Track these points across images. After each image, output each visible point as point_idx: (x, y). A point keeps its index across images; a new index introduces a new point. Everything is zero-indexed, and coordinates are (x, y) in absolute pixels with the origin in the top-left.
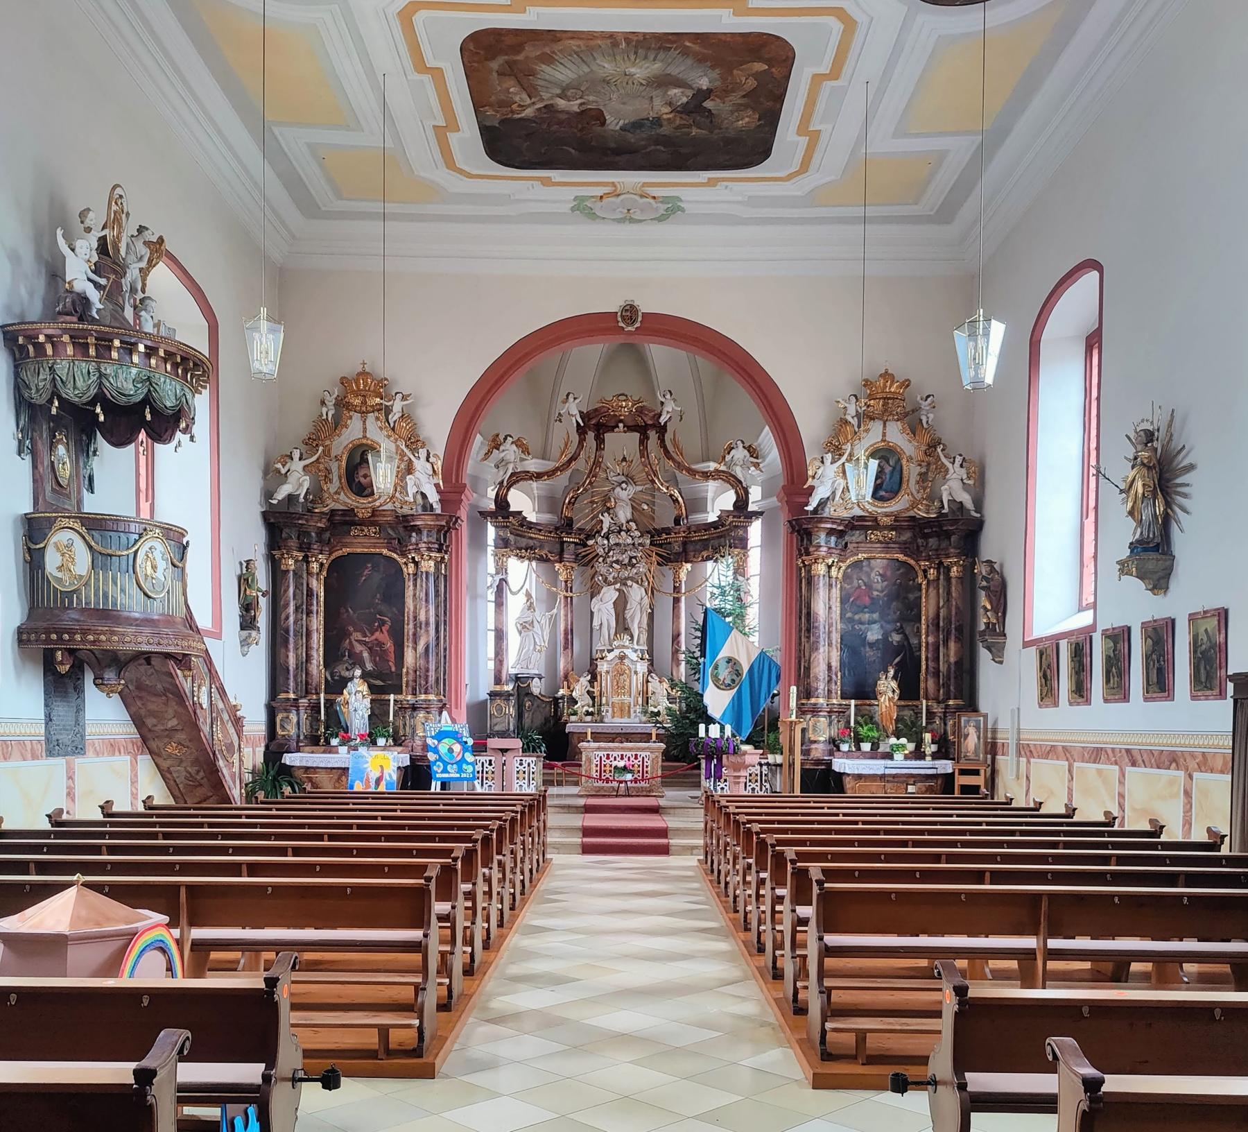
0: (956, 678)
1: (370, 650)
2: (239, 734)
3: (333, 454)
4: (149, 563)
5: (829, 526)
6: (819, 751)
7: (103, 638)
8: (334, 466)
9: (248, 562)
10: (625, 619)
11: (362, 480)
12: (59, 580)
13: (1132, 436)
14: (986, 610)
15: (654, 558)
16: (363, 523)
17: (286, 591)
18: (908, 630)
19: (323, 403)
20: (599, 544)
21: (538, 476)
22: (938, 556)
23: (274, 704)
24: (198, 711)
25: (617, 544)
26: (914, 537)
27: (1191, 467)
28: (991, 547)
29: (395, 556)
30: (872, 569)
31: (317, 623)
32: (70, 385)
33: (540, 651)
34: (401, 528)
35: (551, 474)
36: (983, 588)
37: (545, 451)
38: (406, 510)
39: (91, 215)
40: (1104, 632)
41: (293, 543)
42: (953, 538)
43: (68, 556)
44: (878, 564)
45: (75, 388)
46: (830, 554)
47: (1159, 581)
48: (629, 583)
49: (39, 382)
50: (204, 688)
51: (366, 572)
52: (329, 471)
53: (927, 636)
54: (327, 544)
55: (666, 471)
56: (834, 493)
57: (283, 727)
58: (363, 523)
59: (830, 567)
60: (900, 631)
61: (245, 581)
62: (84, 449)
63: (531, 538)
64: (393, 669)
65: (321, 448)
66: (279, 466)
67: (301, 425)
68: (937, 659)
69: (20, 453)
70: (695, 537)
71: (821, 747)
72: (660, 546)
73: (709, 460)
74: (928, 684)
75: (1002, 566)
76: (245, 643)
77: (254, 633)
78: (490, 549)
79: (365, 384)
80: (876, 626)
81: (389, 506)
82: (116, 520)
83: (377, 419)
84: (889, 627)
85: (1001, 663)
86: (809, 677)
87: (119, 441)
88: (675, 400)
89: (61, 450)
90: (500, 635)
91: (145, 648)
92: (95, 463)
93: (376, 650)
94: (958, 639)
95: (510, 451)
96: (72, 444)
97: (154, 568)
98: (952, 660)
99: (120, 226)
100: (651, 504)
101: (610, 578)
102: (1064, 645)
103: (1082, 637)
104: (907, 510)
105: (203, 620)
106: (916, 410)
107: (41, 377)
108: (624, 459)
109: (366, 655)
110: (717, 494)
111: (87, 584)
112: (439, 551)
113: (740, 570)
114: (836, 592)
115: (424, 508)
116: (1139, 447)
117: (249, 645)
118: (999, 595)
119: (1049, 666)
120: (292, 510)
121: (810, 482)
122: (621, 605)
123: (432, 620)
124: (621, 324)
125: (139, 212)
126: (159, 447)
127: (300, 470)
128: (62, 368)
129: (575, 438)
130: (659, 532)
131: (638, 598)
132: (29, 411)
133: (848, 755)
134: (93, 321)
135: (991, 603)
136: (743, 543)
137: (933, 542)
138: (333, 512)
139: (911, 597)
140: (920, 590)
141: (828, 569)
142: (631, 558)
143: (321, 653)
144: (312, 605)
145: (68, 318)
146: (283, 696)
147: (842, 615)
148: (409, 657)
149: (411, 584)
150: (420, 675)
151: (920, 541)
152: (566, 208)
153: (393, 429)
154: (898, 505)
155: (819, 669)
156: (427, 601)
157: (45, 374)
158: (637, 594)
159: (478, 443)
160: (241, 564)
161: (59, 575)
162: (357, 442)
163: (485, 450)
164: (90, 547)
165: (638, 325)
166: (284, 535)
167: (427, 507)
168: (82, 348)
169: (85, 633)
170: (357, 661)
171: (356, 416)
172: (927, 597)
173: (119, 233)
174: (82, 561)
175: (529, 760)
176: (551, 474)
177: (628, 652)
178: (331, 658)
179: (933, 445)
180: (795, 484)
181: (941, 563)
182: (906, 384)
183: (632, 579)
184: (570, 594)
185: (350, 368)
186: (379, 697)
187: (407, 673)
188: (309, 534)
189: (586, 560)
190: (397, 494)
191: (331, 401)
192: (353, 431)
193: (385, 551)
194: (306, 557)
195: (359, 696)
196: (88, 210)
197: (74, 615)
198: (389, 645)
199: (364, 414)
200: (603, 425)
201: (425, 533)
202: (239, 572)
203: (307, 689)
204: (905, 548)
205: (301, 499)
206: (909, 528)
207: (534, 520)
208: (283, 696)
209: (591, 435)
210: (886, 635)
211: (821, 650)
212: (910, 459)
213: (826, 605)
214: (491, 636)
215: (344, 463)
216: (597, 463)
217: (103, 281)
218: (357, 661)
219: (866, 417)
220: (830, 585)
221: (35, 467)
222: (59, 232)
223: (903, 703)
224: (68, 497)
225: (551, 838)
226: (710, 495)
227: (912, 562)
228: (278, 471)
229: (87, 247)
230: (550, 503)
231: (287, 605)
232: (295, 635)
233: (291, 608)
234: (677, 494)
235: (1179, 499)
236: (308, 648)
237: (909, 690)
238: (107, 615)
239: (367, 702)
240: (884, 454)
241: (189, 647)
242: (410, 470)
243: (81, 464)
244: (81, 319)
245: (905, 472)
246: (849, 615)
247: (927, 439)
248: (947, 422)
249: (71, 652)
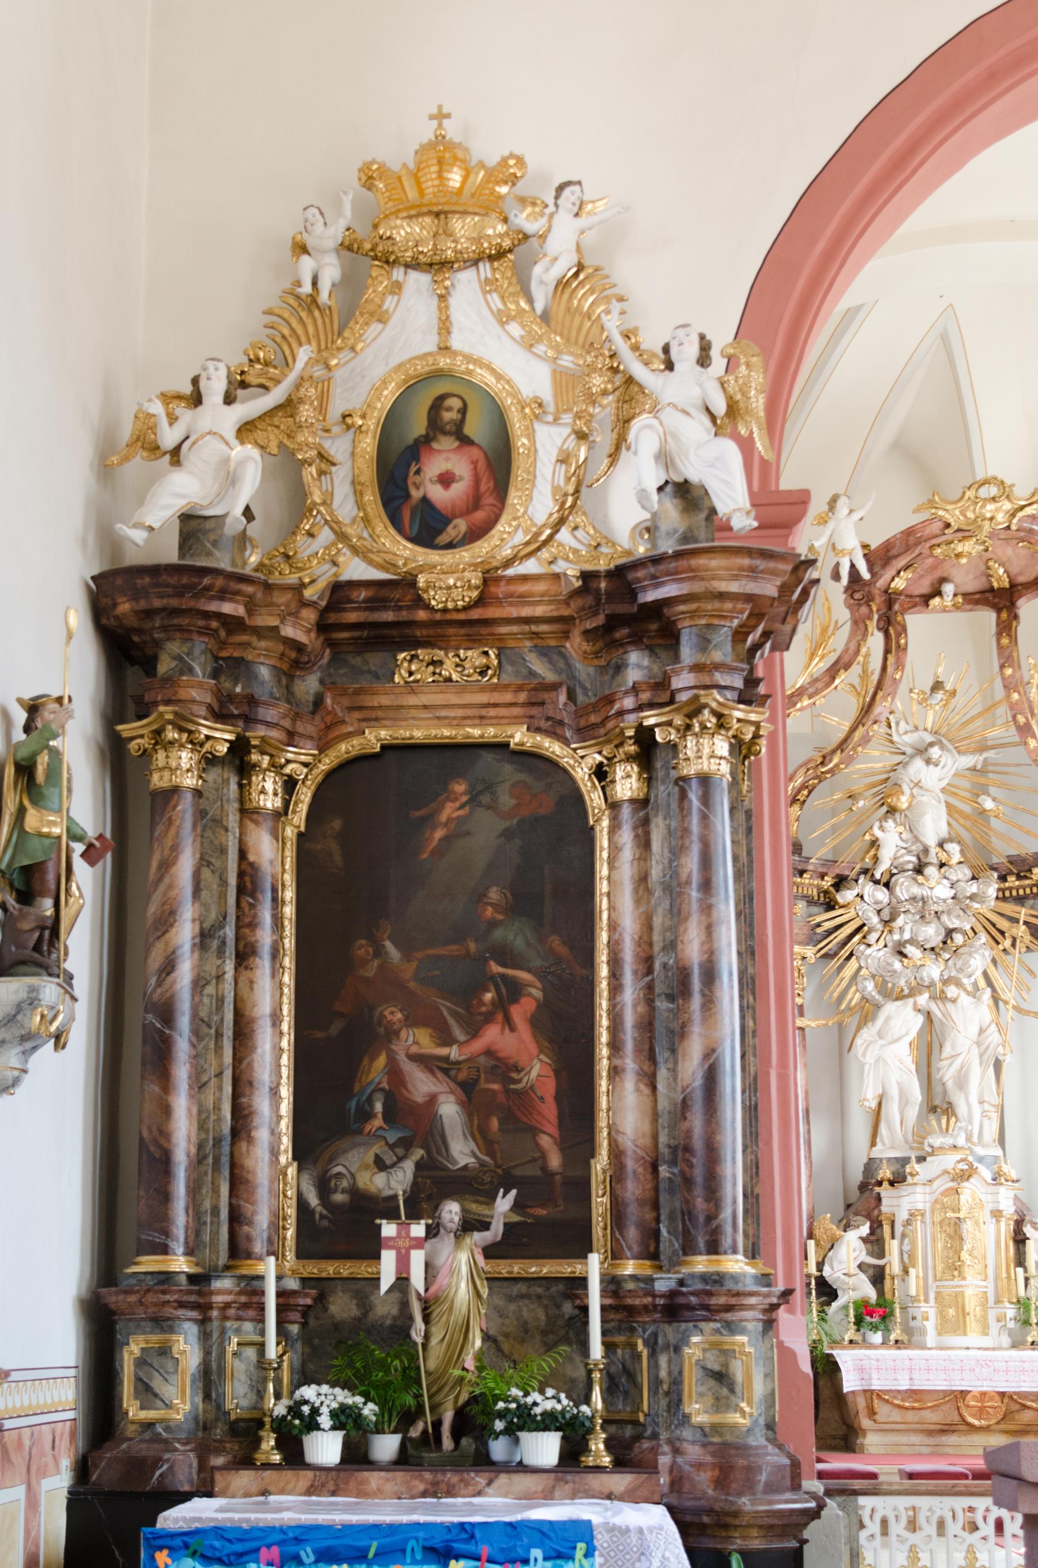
1: (468, 1092)
3: (337, 407)
9: (33, 708)
11: (438, 494)
17: (167, 865)
20: (864, 900)
23: (113, 1298)
31: (273, 992)
41: (197, 690)
51: (449, 811)
57: (146, 1392)
67: (220, 332)
77: (49, 990)
83: (488, 286)
109: (449, 1110)
123: (729, 961)
131: (974, 1030)
142: (950, 933)
144: (253, 925)
148: (623, 1110)
158: (969, 1017)
162: (422, 368)
166: (165, 665)
171: (417, 282)
178: (323, 1120)
192: (404, 331)
193: (519, 736)
194: (239, 748)
208: (148, 1264)
218: (416, 1127)
231: (167, 920)
232: (196, 1033)
233: (185, 932)
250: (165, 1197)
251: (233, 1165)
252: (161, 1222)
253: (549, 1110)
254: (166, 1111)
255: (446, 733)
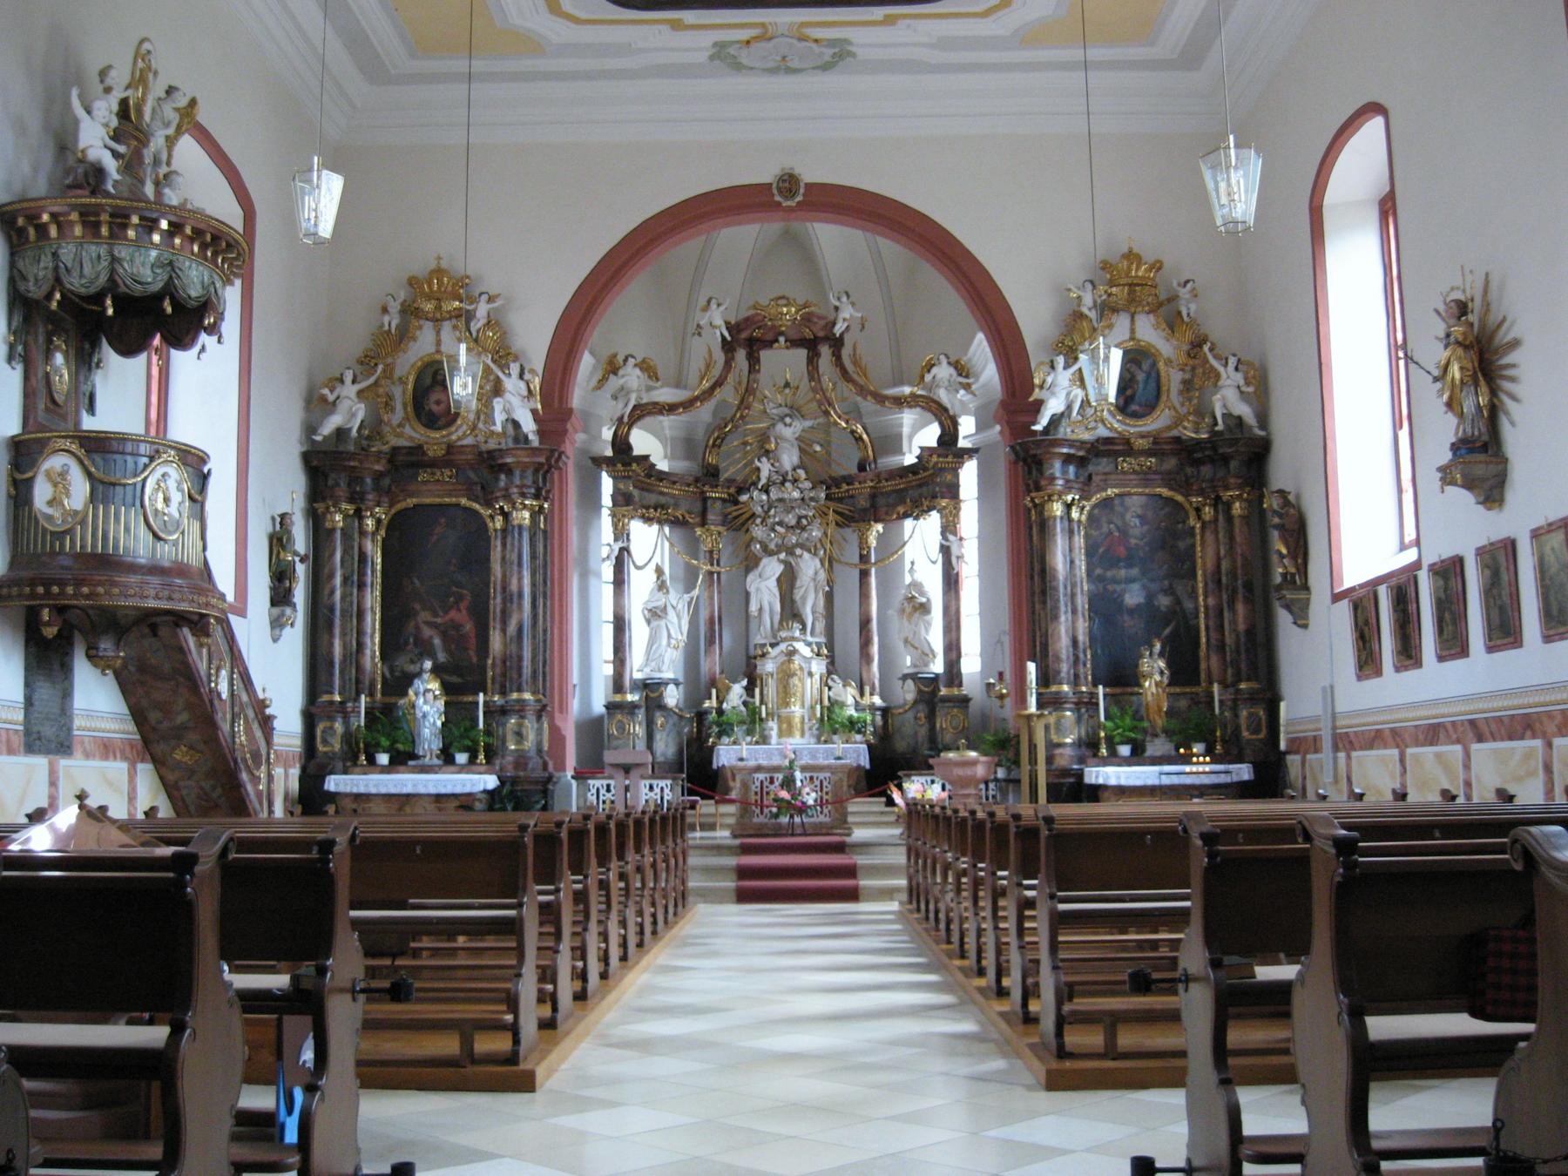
0: (1247, 650)
2: (269, 742)
3: (398, 373)
4: (161, 495)
5: (1065, 450)
6: (1065, 757)
7: (101, 590)
8: (397, 391)
10: (793, 601)
12: (49, 518)
13: (1442, 308)
14: (1282, 556)
15: (831, 515)
16: (434, 464)
17: (332, 555)
18: (1180, 589)
19: (385, 310)
21: (671, 408)
22: (1214, 488)
24: (216, 702)
25: (781, 500)
26: (1180, 468)
27: (1515, 344)
28: (1281, 474)
29: (477, 506)
30: (1127, 509)
31: (373, 599)
32: (76, 274)
33: (676, 648)
34: (487, 469)
35: (688, 405)
36: (1276, 527)
37: (680, 372)
38: (492, 445)
39: (113, 73)
40: (1432, 568)
41: (342, 491)
42: (1233, 464)
43: (62, 487)
44: (1135, 506)
45: (82, 276)
46: (1068, 488)
47: (1491, 490)
48: (798, 551)
49: (38, 271)
50: (224, 673)
51: (438, 530)
52: (390, 397)
53: (1206, 597)
54: (387, 494)
55: (844, 400)
56: (1069, 407)
58: (434, 464)
59: (1069, 506)
60: (1170, 591)
61: (279, 540)
62: (85, 361)
63: (662, 493)
64: (475, 660)
65: (380, 367)
66: (326, 391)
68: (1220, 628)
69: (10, 359)
70: (888, 486)
71: (1068, 752)
72: (840, 500)
73: (901, 383)
74: (1209, 662)
75: (1298, 497)
76: (277, 624)
78: (605, 513)
79: (440, 283)
80: (1136, 587)
81: (469, 441)
82: (122, 438)
83: (455, 327)
84: (1154, 587)
85: (1305, 626)
86: (1047, 656)
87: (128, 349)
88: (853, 304)
89: (59, 359)
90: (620, 625)
91: (152, 604)
92: (98, 378)
93: (451, 635)
94: (1249, 601)
95: (632, 377)
96: (72, 352)
97: (167, 500)
98: (1241, 627)
99: (146, 88)
100: (826, 445)
101: (772, 546)
102: (1383, 591)
103: (1403, 578)
104: (1169, 428)
105: (225, 581)
106: (1173, 299)
107: (42, 265)
108: (787, 385)
110: (916, 429)
111: (83, 522)
112: (537, 497)
113: (949, 528)
114: (1079, 541)
115: (516, 440)
116: (1452, 321)
117: (282, 626)
118: (1298, 535)
119: (1366, 623)
120: (341, 449)
121: (1037, 394)
122: (788, 581)
124: (778, 198)
125: (168, 70)
126: (176, 355)
127: (353, 394)
128: (67, 252)
129: (719, 357)
130: (836, 482)
132: (24, 306)
133: (1105, 762)
134: (107, 195)
135: (1288, 548)
136: (953, 491)
137: (1206, 470)
138: (396, 450)
139: (1182, 545)
140: (1193, 535)
141: (1066, 508)
143: (377, 640)
145: (79, 192)
146: (325, 698)
147: (1089, 573)
148: (496, 643)
149: (499, 543)
150: (511, 664)
151: (1189, 470)
152: (702, 57)
153: (476, 340)
154: (1157, 422)
155: (1062, 644)
156: (520, 565)
157: (47, 261)
159: (587, 364)
160: (273, 519)
161: (49, 511)
163: (599, 375)
164: (89, 475)
165: (799, 198)
166: (330, 482)
167: (520, 437)
168: (92, 227)
169: (79, 583)
170: (426, 650)
172: (1203, 544)
173: (144, 94)
174: (80, 489)
175: (662, 783)
176: (688, 405)
177: (800, 646)
179: (1197, 344)
180: (1018, 401)
181: (1218, 498)
182: (1157, 266)
183: (802, 546)
184: (715, 568)
185: (420, 265)
186: (454, 698)
187: (494, 664)
188: (360, 480)
189: (739, 523)
190: (481, 425)
191: (395, 307)
192: (423, 344)
193: (464, 501)
195: (430, 696)
196: (110, 67)
197: (67, 562)
198: (469, 627)
199: (437, 321)
200: (758, 340)
201: (517, 473)
202: (270, 529)
203: (358, 685)
204: (1169, 480)
205: (354, 433)
206: (1174, 453)
207: (666, 469)
209: (741, 355)
210: (1150, 598)
211: (1063, 618)
212: (1169, 362)
213: (1066, 557)
214: (608, 632)
215: (410, 387)
216: (749, 391)
217: (122, 149)
219: (1107, 309)
220: (1071, 532)
221: (27, 378)
222: (75, 93)
223: (1178, 690)
224: (64, 417)
225: (693, 860)
226: (906, 430)
227: (1179, 498)
228: (324, 399)
229: (106, 109)
230: (686, 446)
231: (332, 576)
232: (343, 616)
233: (338, 580)
234: (860, 429)
235: (1506, 385)
236: (360, 633)
237: (1183, 670)
238: (107, 563)
239: (441, 704)
240: (1136, 358)
241: (207, 605)
242: (498, 390)
243: (82, 378)
244: (93, 193)
245: (1164, 380)
246: (1098, 571)
247: (1189, 336)
248: (1212, 313)
249: (60, 610)
250: (332, 674)
251: (358, 663)
252: (332, 686)
253: (473, 642)
254: (331, 644)
255: (438, 500)
